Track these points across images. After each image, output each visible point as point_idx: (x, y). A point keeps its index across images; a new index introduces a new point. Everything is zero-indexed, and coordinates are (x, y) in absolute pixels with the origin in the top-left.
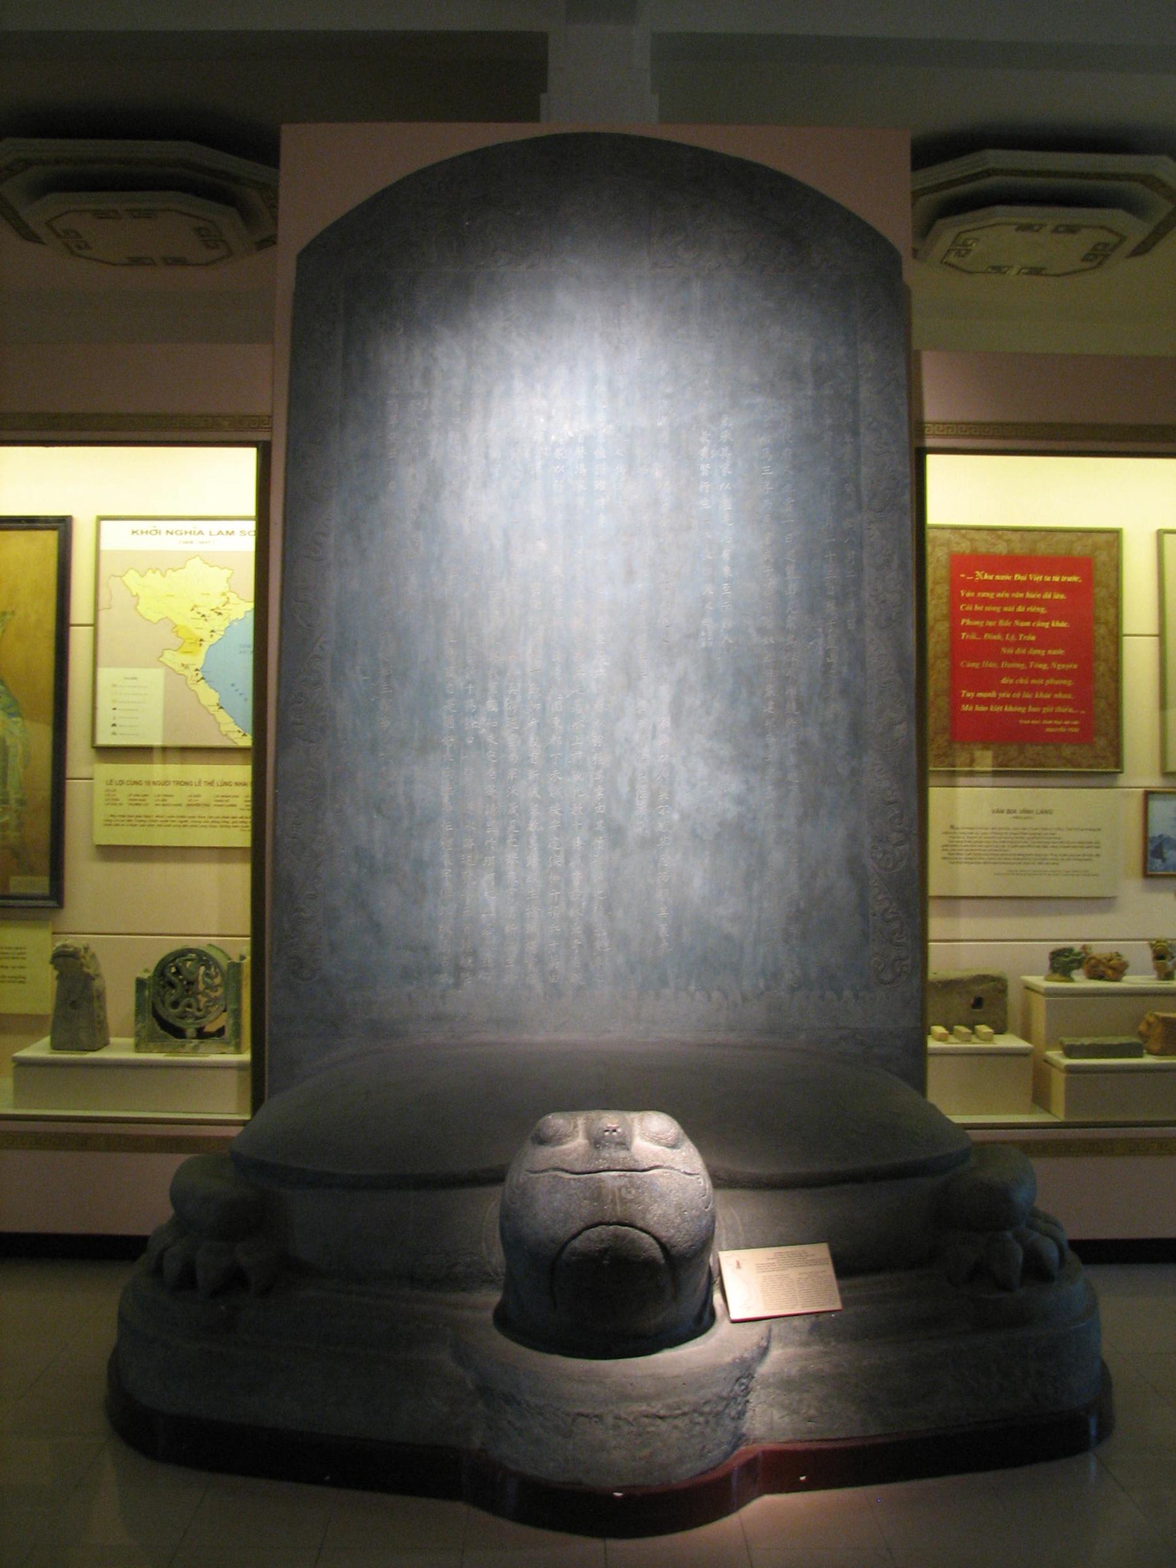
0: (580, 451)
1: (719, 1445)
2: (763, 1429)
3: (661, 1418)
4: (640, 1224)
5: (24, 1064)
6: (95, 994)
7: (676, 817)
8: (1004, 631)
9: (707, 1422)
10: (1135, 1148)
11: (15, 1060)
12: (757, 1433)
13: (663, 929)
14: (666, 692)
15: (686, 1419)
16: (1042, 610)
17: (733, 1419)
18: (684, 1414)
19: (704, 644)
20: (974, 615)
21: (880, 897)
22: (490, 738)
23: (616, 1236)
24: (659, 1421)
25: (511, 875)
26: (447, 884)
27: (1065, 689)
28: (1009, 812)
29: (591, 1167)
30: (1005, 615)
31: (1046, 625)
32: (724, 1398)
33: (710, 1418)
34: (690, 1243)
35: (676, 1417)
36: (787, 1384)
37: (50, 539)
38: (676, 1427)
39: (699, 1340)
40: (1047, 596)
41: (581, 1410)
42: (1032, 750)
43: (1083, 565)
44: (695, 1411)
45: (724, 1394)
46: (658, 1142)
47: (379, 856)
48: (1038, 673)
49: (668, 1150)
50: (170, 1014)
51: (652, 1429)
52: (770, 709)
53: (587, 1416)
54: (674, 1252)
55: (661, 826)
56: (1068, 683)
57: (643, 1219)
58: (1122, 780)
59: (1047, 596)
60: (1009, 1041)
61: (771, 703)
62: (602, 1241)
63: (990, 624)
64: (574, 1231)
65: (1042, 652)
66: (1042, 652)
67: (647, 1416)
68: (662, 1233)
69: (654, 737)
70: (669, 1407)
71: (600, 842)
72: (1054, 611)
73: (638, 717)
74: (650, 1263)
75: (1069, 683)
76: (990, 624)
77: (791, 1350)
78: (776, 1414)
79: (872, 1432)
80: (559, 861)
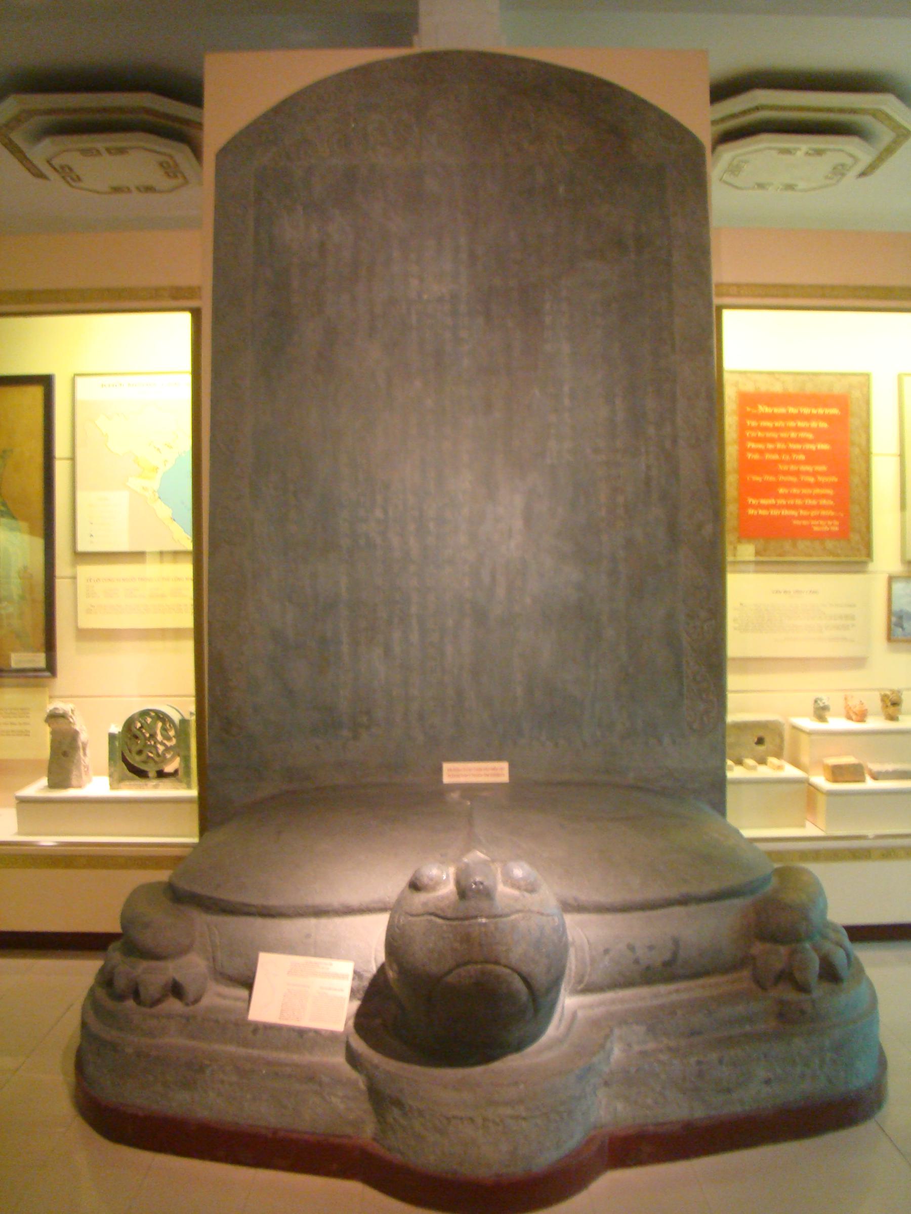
5: (23, 802)
7: (528, 600)
8: (779, 452)
10: (888, 854)
11: (17, 798)
13: (519, 691)
14: (519, 501)
16: (810, 436)
20: (757, 440)
22: (379, 540)
25: (397, 649)
27: (825, 496)
28: (785, 592)
30: (780, 440)
31: (812, 447)
40: (814, 424)
42: (802, 545)
43: (841, 401)
48: (808, 485)
49: (526, 894)
50: (136, 760)
52: (603, 513)
53: (461, 1119)
56: (830, 492)
58: (871, 567)
59: (814, 424)
60: (790, 771)
63: (770, 446)
65: (809, 468)
66: (809, 468)
71: (467, 622)
72: (819, 435)
75: (830, 492)
76: (770, 446)
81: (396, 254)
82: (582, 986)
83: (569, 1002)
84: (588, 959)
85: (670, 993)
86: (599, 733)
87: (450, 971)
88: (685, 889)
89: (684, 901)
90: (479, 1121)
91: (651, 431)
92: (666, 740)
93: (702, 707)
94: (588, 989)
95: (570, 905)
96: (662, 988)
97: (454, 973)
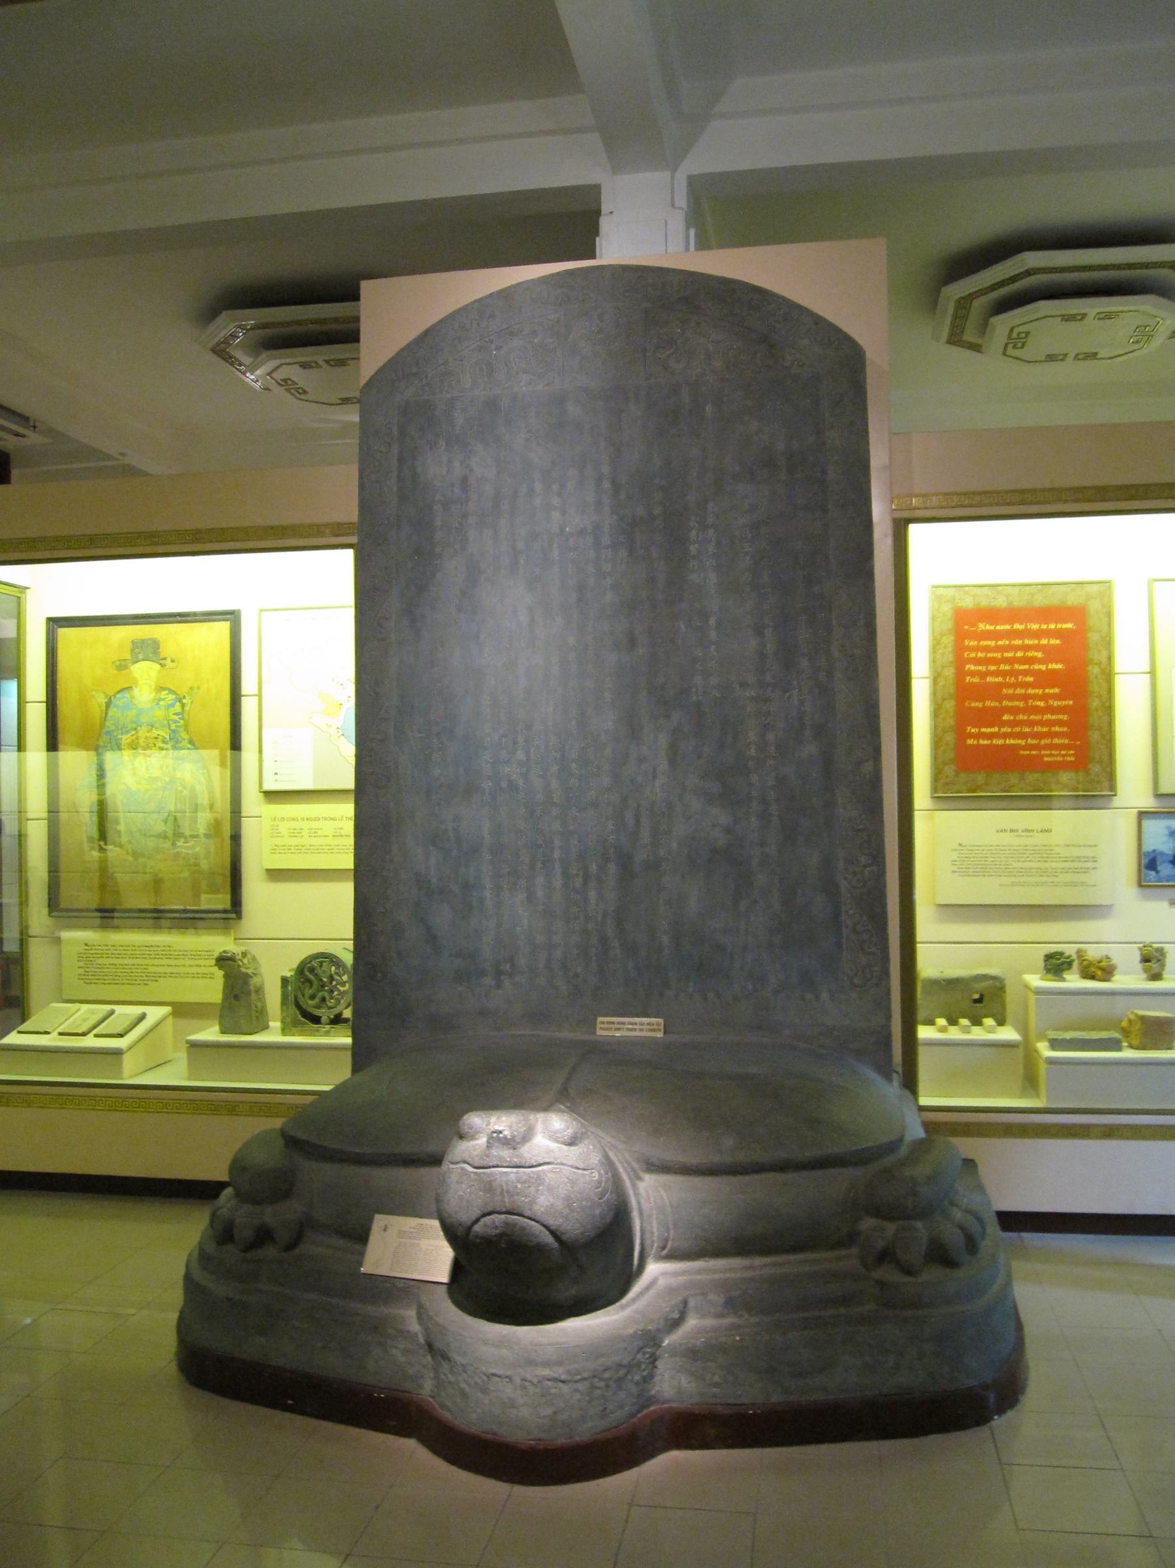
0: (589, 540)
1: (621, 1407)
3: (563, 1382)
4: (528, 1213)
5: (194, 1046)
6: (252, 988)
7: (674, 845)
8: (1004, 674)
9: (608, 1386)
10: (1110, 1132)
11: (188, 1042)
12: (666, 1395)
13: (665, 940)
14: (663, 740)
15: (587, 1384)
16: (1039, 655)
17: (637, 1384)
18: (584, 1379)
19: (695, 698)
20: (977, 661)
21: (851, 912)
22: (521, 782)
23: (506, 1224)
24: (561, 1385)
25: (540, 893)
26: (489, 903)
27: (1060, 723)
28: (1012, 831)
29: (484, 1163)
30: (1005, 661)
31: (1043, 667)
32: (624, 1366)
33: (611, 1383)
34: (582, 1230)
35: (577, 1381)
37: (224, 627)
38: (577, 1390)
39: (593, 1314)
40: (1044, 642)
41: (494, 1371)
42: (1032, 777)
43: (1077, 614)
44: (594, 1377)
45: (625, 1362)
46: (557, 1142)
47: (434, 880)
48: (1038, 710)
49: (565, 1148)
50: (309, 1005)
51: (553, 1391)
52: (752, 752)
53: (499, 1376)
54: (564, 1238)
55: (662, 853)
56: (1065, 717)
58: (1117, 801)
59: (1044, 642)
60: (1008, 1034)
61: (753, 746)
62: (497, 1227)
63: (992, 668)
64: (474, 1218)
65: (1039, 692)
66: (1039, 692)
68: (552, 1222)
69: (654, 777)
70: (568, 1372)
71: (612, 868)
72: (1051, 654)
73: (642, 760)
74: (540, 1248)
75: (1065, 717)
76: (992, 668)
77: (710, 1322)
78: (685, 1381)
79: (775, 1399)
80: (578, 882)
81: (538, 486)
82: (665, 1252)
83: (653, 1268)
84: (671, 1223)
85: (765, 1266)
86: (750, 987)
87: (477, 1221)
88: (782, 1155)
89: (781, 1167)
90: (518, 1380)
91: (805, 663)
92: (825, 995)
93: (863, 960)
94: (672, 1256)
95: (653, 1165)
96: (758, 1261)
97: (480, 1223)
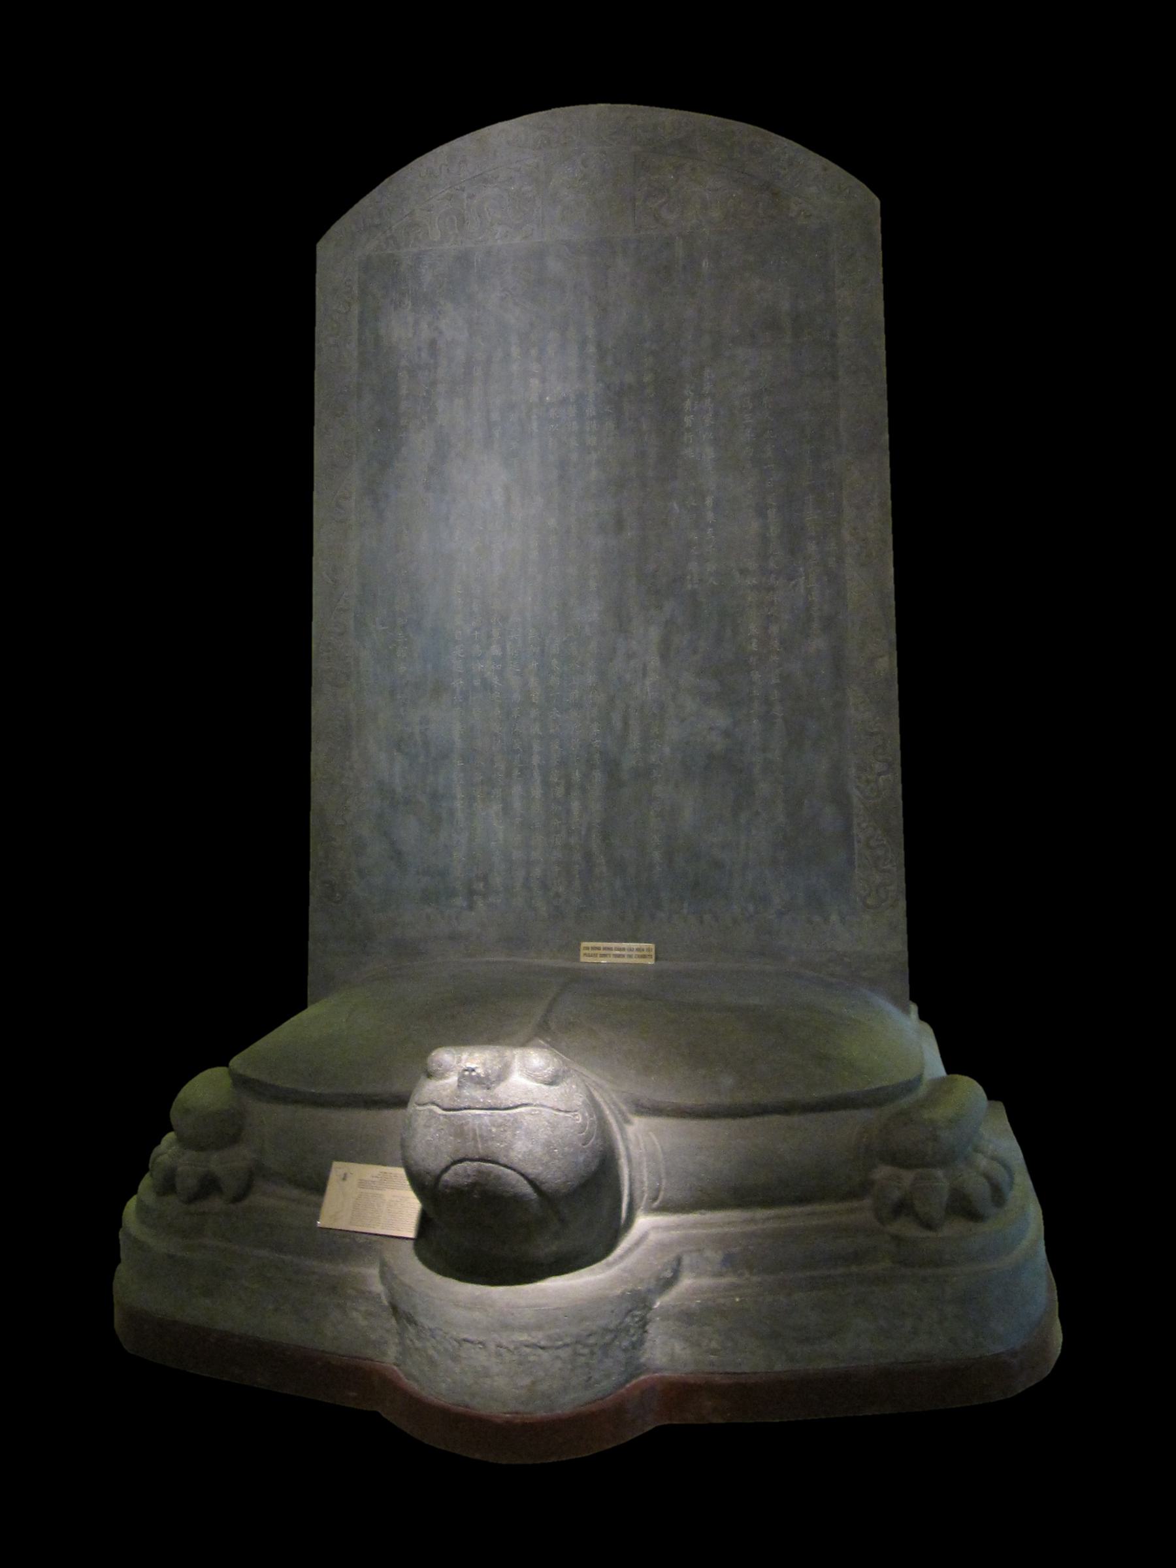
0: (572, 410)
1: (608, 1376)
2: (664, 1360)
3: (543, 1348)
4: (503, 1160)
7: (667, 750)
9: (592, 1353)
12: (658, 1362)
13: (657, 855)
14: (655, 633)
15: (569, 1350)
17: (625, 1350)
18: (566, 1345)
19: (689, 587)
21: (864, 825)
22: (495, 680)
23: (480, 1172)
24: (541, 1351)
25: (517, 805)
26: (460, 815)
29: (455, 1105)
32: (611, 1331)
33: (596, 1349)
34: (563, 1179)
35: (558, 1348)
36: (686, 1317)
38: (558, 1357)
39: (577, 1273)
41: (465, 1336)
44: (577, 1342)
45: (612, 1326)
46: (535, 1079)
47: (399, 789)
51: (532, 1358)
52: (754, 646)
53: (472, 1342)
54: (544, 1188)
55: (653, 759)
57: (506, 1156)
61: (755, 641)
62: (469, 1176)
64: (443, 1165)
67: (527, 1346)
68: (530, 1170)
69: (645, 675)
70: (549, 1337)
71: (598, 776)
73: (630, 656)
74: (517, 1200)
77: (706, 1282)
78: (678, 1347)
79: (778, 1367)
80: (560, 791)
81: (515, 351)
82: (656, 1204)
83: (643, 1222)
84: (663, 1171)
85: (768, 1219)
86: (751, 908)
87: (447, 1168)
88: (787, 1095)
89: (786, 1109)
90: (492, 1347)
91: (812, 547)
92: (834, 918)
93: (878, 878)
94: (664, 1209)
95: (643, 1106)
96: (760, 1213)
97: (451, 1172)
